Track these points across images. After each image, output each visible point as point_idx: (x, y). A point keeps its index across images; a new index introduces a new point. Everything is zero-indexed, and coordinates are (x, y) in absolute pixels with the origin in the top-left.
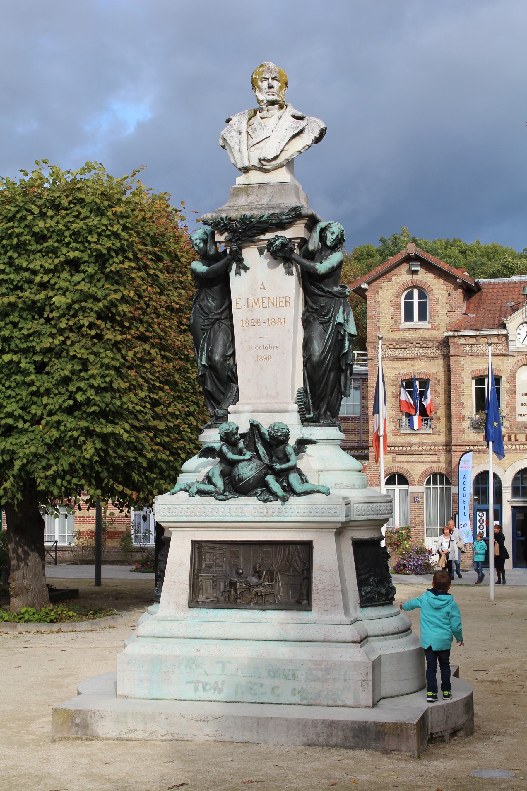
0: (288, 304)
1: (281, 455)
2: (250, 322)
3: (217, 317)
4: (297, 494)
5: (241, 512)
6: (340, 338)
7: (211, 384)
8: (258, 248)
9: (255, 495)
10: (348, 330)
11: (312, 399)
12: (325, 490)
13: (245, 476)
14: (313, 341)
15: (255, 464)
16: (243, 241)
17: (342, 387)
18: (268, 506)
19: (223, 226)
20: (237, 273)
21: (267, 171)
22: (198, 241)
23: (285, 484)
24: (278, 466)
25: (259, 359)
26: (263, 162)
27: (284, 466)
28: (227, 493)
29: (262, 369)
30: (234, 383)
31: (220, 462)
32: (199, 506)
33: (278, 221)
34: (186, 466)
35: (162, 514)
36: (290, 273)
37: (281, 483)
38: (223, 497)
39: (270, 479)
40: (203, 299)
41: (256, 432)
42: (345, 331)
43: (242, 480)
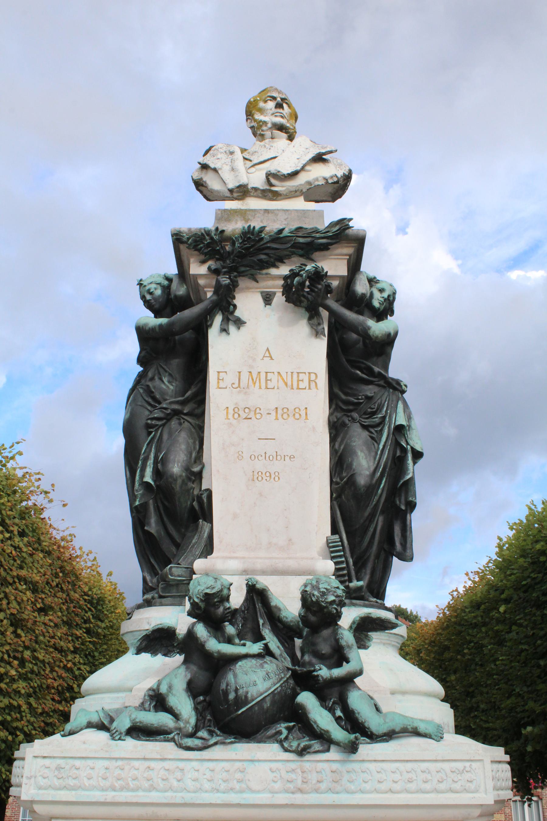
0: (313, 384)
1: (325, 648)
2: (241, 412)
3: (176, 407)
4: (372, 737)
5: (239, 781)
6: (398, 453)
7: (157, 523)
8: (262, 293)
9: (275, 738)
10: (411, 442)
11: (352, 557)
12: (430, 730)
13: (253, 692)
14: (355, 453)
15: (270, 666)
16: (241, 274)
17: (398, 544)
18: (307, 765)
19: (208, 245)
20: (224, 330)
21: (275, 196)
22: (153, 286)
23: (339, 713)
24: (324, 672)
25: (256, 477)
26: (273, 181)
27: (337, 672)
28: (203, 733)
29: (261, 494)
30: (205, 520)
31: (185, 662)
32: (136, 764)
33: (309, 240)
34: (94, 681)
35: (42, 782)
36: (317, 334)
37: (331, 710)
38: (197, 742)
39: (307, 699)
40: (152, 379)
41: (259, 606)
42: (408, 444)
43: (246, 701)
